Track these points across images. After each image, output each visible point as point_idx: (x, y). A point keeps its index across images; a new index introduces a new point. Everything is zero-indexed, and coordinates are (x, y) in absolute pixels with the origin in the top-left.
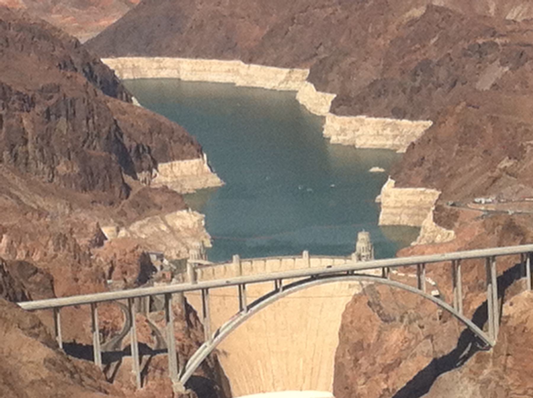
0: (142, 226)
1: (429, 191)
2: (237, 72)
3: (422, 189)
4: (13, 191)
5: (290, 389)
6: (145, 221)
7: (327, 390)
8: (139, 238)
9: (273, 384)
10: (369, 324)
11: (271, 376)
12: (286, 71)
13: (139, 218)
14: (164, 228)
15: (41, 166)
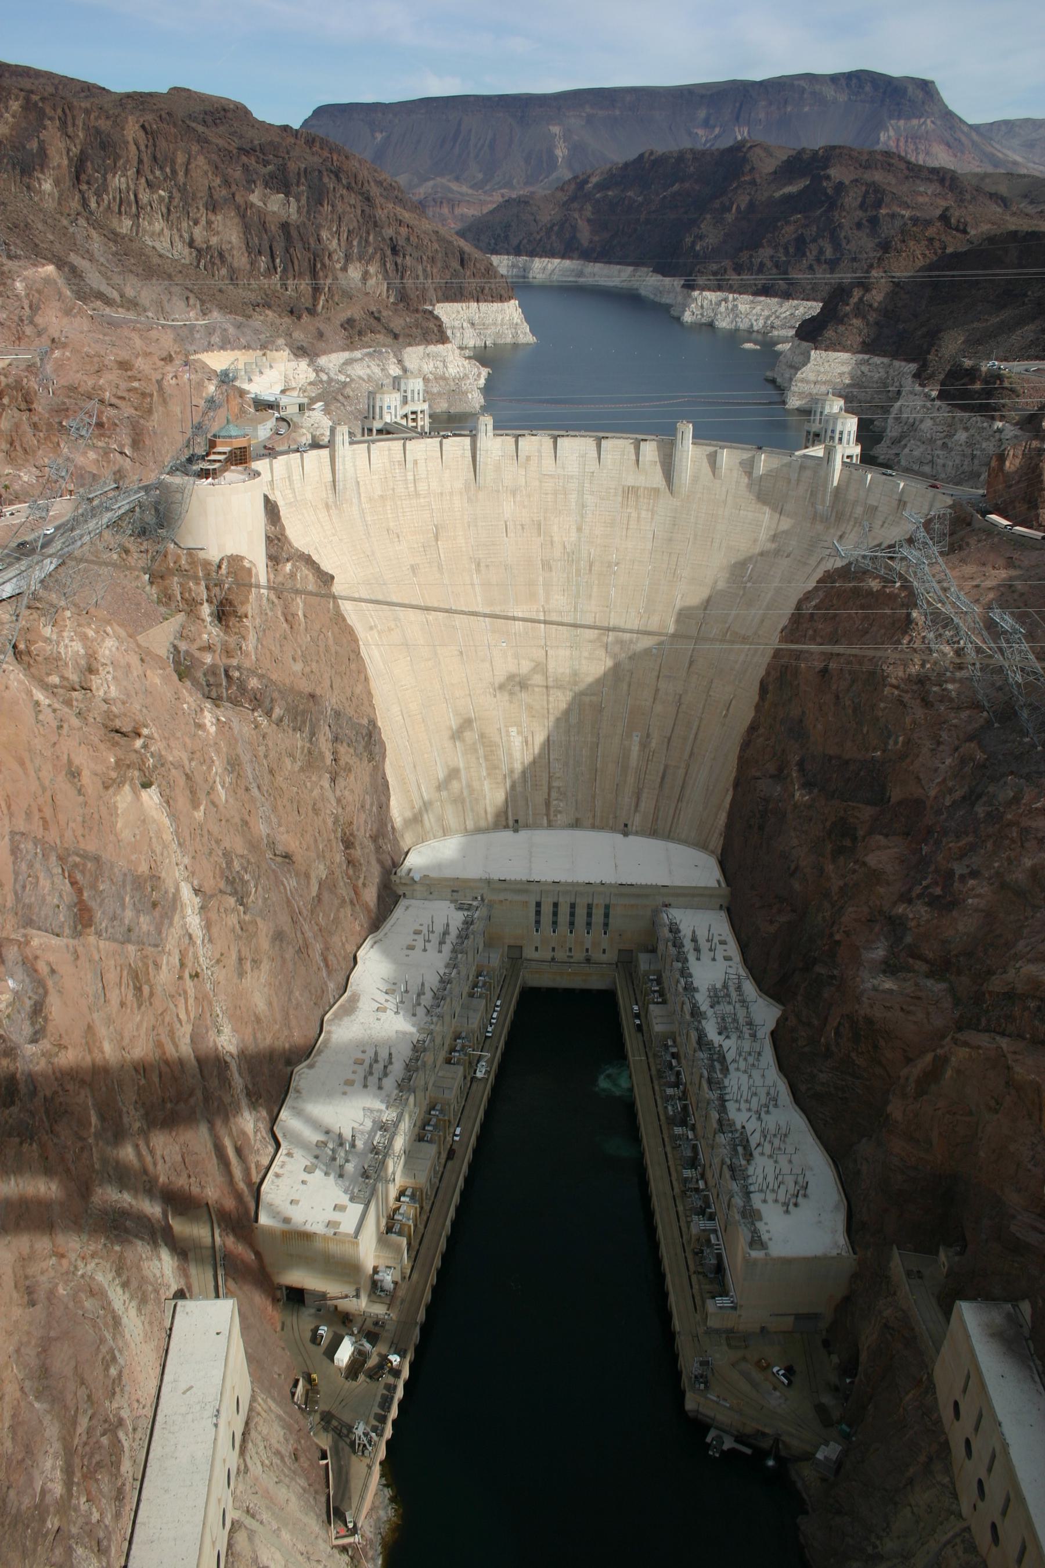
0: (348, 362)
1: (877, 360)
2: (581, 274)
3: (866, 357)
4: (74, 259)
5: (593, 827)
6: (358, 354)
7: (703, 846)
8: (330, 380)
9: (548, 804)
10: (919, 713)
11: (545, 776)
12: (631, 268)
13: (350, 346)
14: (394, 370)
15: (159, 225)
